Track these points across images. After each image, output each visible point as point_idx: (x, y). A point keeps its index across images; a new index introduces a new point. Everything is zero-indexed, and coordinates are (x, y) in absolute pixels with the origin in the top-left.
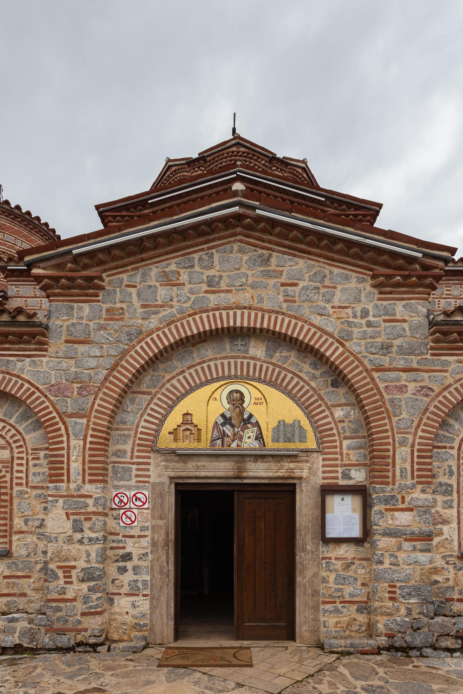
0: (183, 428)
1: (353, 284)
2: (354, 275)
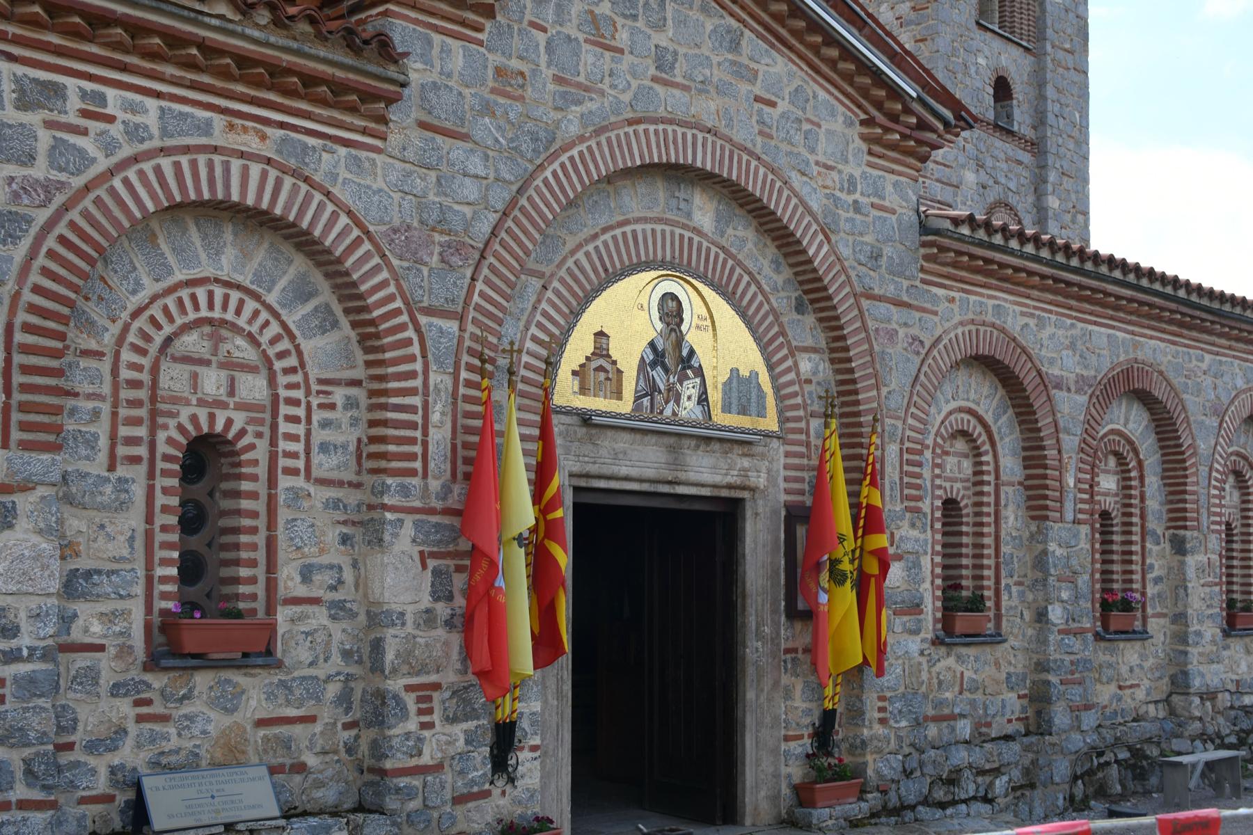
0: (594, 364)
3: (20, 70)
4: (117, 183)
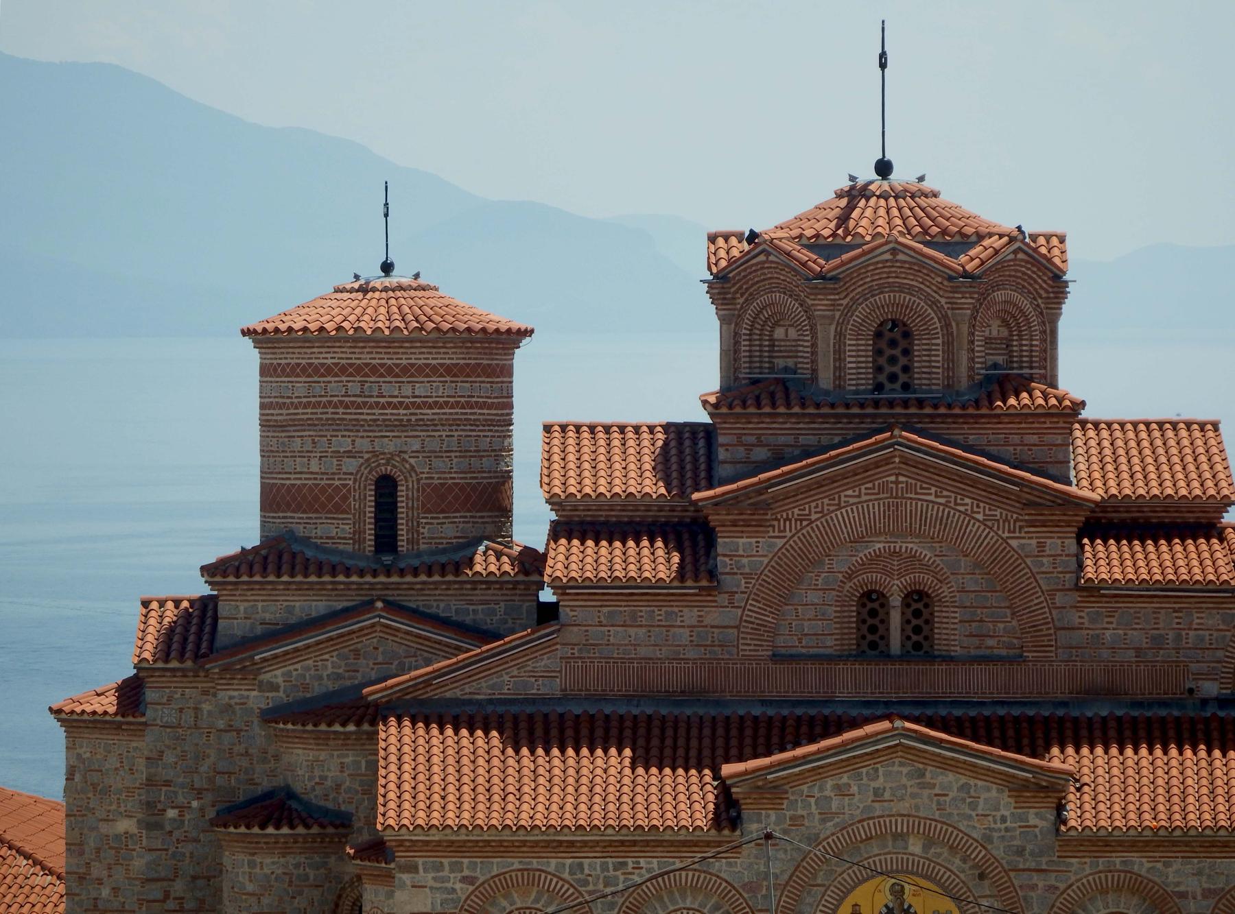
1: (994, 793)
2: (994, 786)
3: (614, 860)
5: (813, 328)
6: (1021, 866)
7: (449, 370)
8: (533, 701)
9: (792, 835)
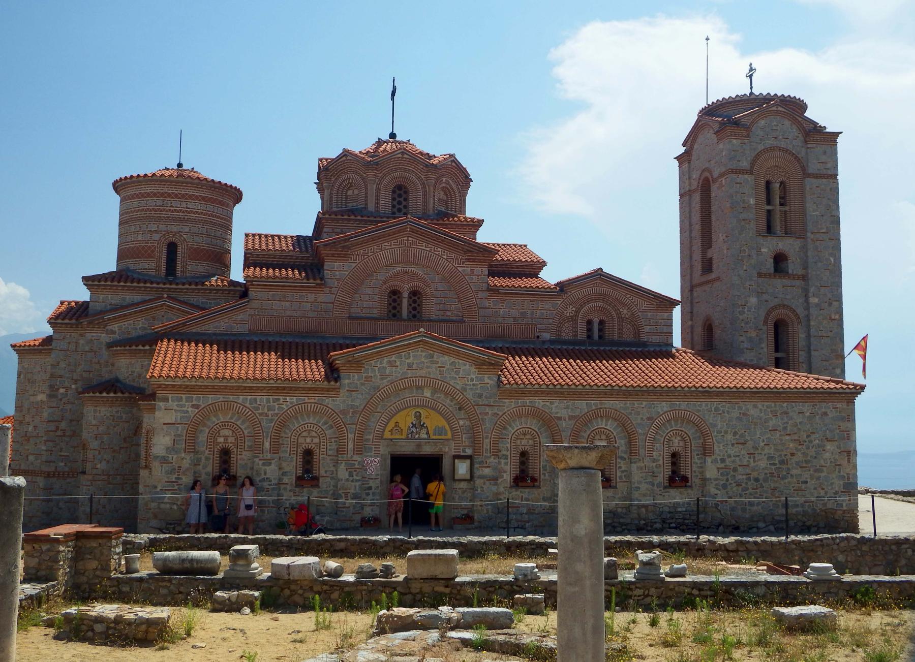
1: (467, 367)
2: (468, 363)
4: (288, 411)
5: (366, 186)
6: (481, 403)
7: (204, 198)
8: (234, 335)
9: (366, 386)
